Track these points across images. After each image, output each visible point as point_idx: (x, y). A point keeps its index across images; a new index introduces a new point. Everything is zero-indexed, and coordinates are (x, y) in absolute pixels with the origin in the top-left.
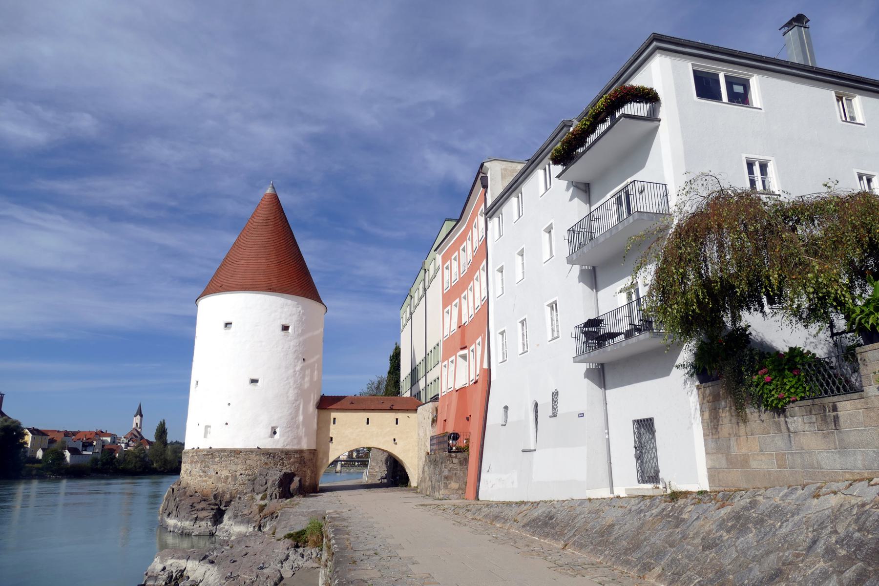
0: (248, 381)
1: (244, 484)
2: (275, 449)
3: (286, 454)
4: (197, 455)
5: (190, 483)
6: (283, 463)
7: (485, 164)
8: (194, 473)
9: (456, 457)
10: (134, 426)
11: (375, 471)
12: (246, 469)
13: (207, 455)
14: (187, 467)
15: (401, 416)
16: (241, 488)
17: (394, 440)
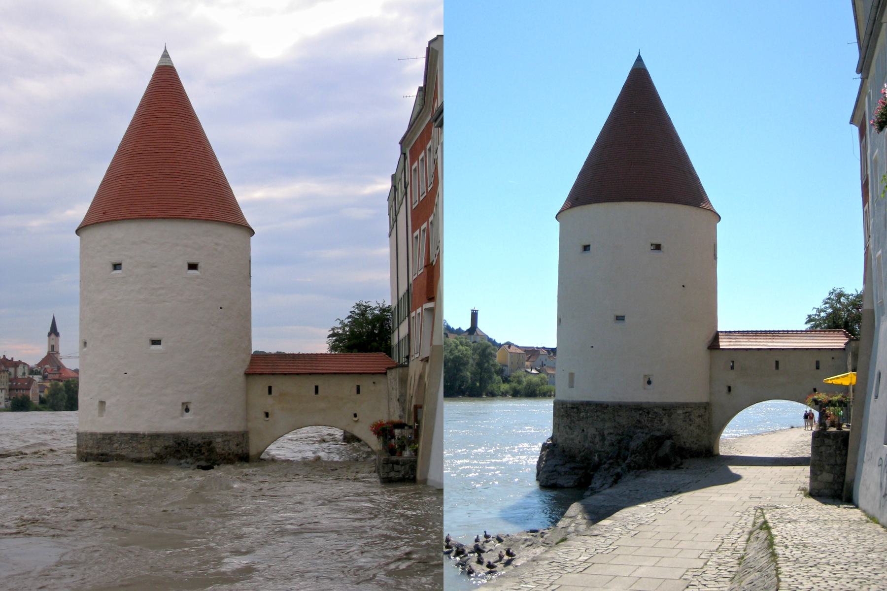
3: (663, 410)
4: (562, 408)
6: (661, 421)
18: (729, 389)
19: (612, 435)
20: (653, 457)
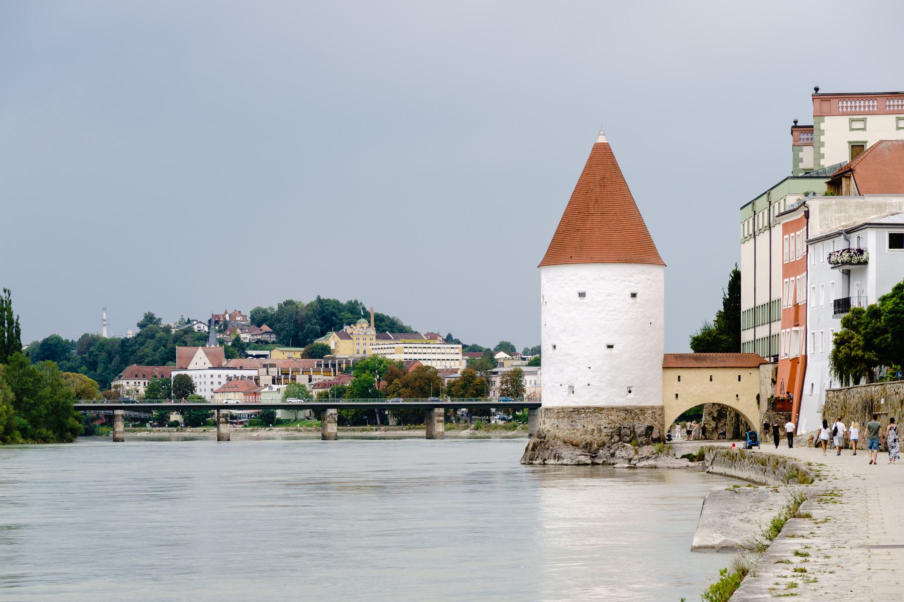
0: (606, 347)
1: (608, 436)
2: (631, 406)
3: (640, 410)
4: (563, 412)
5: (559, 435)
6: (639, 418)
7: (807, 202)
8: (561, 426)
9: (783, 415)
11: (710, 427)
12: (609, 424)
13: (573, 411)
14: (553, 422)
15: (744, 373)
16: (606, 439)
17: (737, 396)
18: (677, 395)
19: (606, 429)
20: (650, 439)
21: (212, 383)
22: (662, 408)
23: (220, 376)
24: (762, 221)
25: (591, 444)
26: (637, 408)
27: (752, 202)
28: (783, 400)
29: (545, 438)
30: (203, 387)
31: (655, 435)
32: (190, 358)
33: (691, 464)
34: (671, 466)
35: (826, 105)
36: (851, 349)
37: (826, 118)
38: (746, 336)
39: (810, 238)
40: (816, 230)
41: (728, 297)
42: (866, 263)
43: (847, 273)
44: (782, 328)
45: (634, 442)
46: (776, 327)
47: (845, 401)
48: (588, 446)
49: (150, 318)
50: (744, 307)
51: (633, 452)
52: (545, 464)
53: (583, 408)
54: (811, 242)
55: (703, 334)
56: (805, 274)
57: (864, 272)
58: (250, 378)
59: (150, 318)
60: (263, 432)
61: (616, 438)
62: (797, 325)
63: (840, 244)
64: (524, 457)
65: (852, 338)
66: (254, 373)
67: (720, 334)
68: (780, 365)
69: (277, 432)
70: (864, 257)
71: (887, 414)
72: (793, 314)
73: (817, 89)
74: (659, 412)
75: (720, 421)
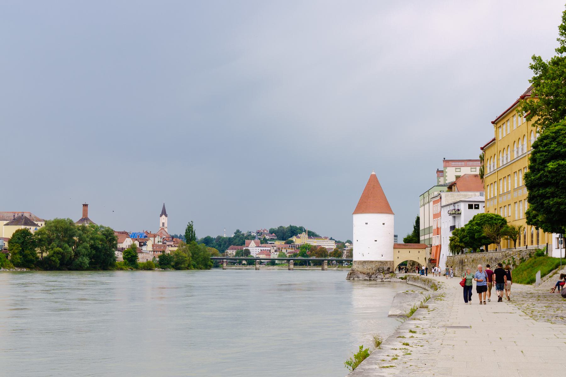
8: (359, 267)
10: (161, 225)
15: (420, 250)
16: (374, 272)
18: (398, 257)
21: (256, 252)
22: (393, 262)
23: (258, 249)
24: (426, 200)
25: (369, 273)
26: (385, 261)
27: (423, 194)
28: (433, 260)
29: (354, 271)
30: (253, 253)
31: (391, 271)
32: (249, 244)
33: (402, 281)
34: (396, 281)
35: (447, 164)
36: (455, 242)
37: (447, 168)
38: (422, 238)
39: (442, 206)
40: (444, 203)
41: (415, 225)
42: (460, 214)
43: (454, 217)
44: (433, 235)
45: (383, 273)
46: (431, 235)
47: (453, 260)
48: (368, 274)
49: (238, 231)
50: (421, 229)
51: (383, 276)
52: (354, 280)
53: (367, 261)
54: (442, 207)
55: (407, 237)
56: (440, 217)
57: (460, 216)
58: (268, 250)
59: (238, 231)
60: (271, 267)
61: (378, 271)
62: (438, 235)
63: (452, 207)
64: (347, 277)
65: (456, 239)
66: (269, 249)
67: (413, 237)
68: (432, 248)
69: (275, 267)
70: (460, 212)
71: (467, 265)
72: (437, 231)
73: (444, 159)
74: (392, 263)
75: (413, 266)
